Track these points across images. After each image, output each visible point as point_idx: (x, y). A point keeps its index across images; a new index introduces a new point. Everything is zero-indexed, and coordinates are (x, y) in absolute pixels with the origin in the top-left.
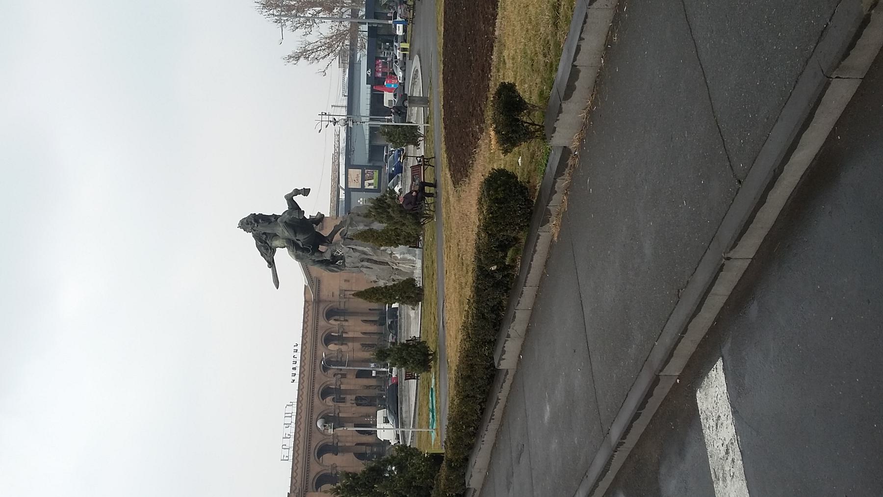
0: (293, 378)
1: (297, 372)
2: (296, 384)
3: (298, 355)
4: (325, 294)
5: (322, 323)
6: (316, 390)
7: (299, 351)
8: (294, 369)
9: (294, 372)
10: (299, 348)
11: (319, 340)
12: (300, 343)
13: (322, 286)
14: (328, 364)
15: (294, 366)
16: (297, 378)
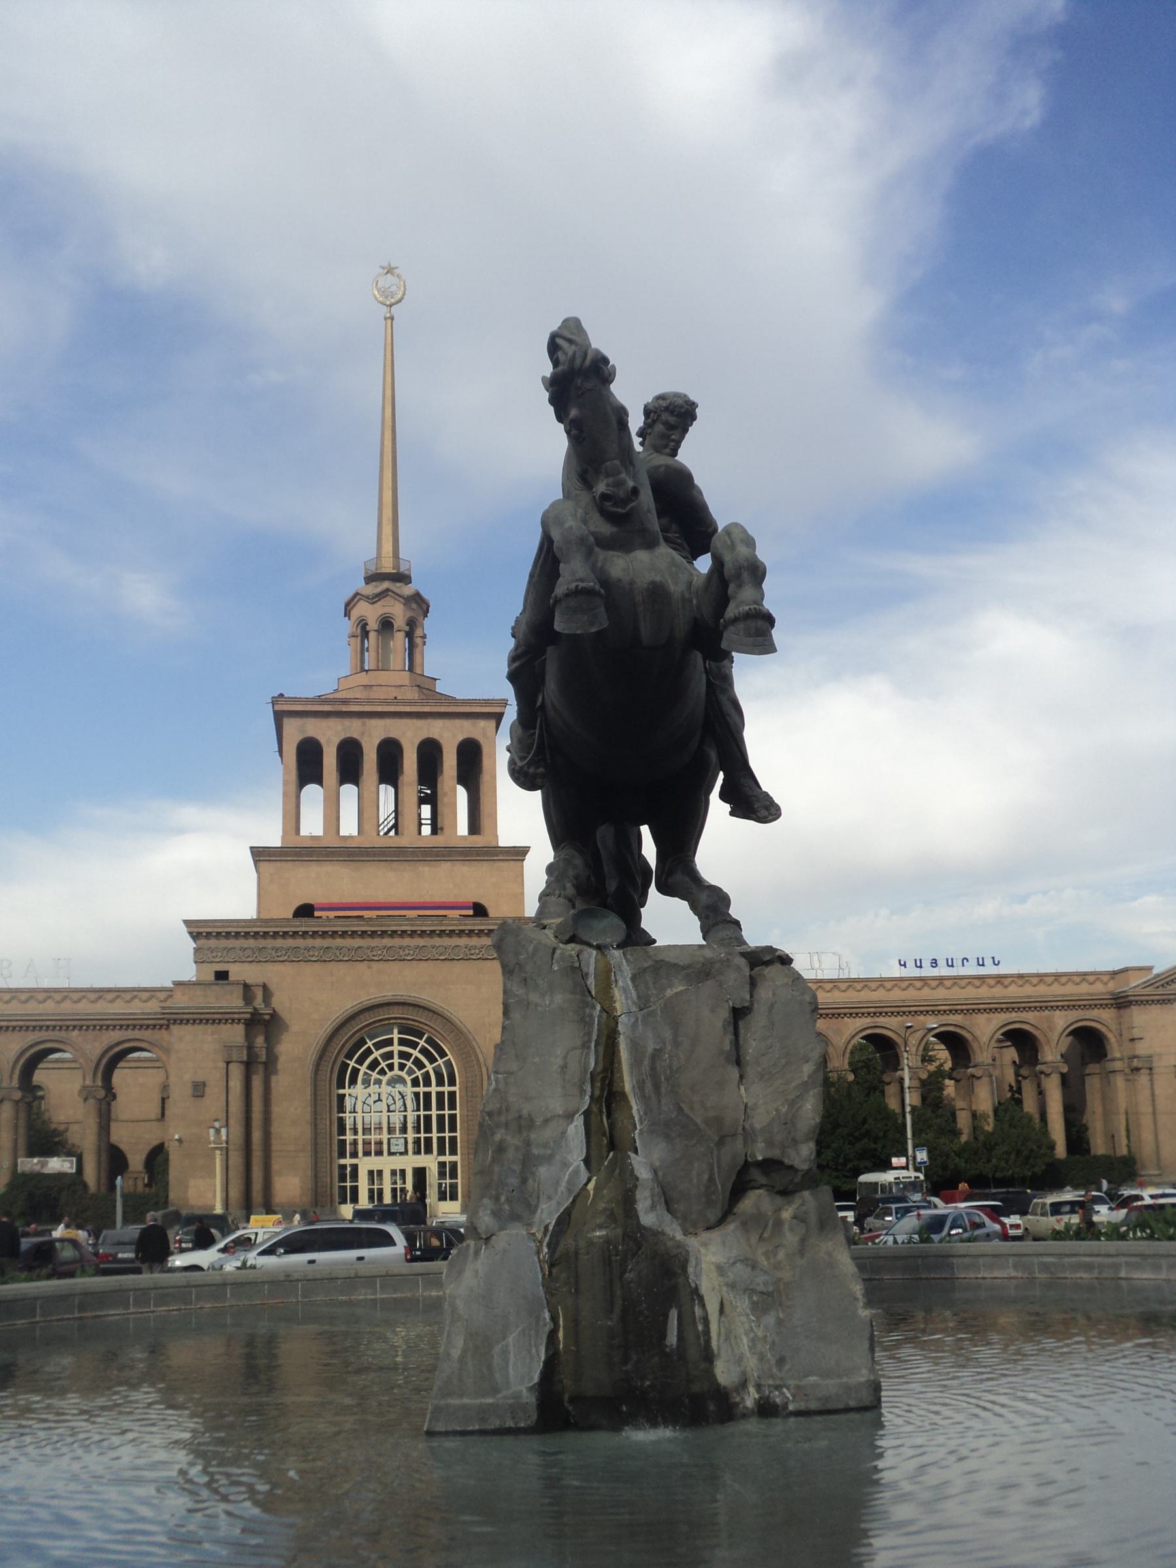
0: (910, 964)
1: (928, 971)
2: (897, 972)
3: (971, 970)
4: (1140, 1017)
5: (1062, 1020)
6: (882, 1020)
7: (982, 971)
8: (934, 963)
9: (926, 964)
10: (989, 970)
11: (1013, 1016)
12: (1002, 970)
13: (1155, 1010)
14: (955, 1042)
15: (942, 963)
16: (911, 972)
